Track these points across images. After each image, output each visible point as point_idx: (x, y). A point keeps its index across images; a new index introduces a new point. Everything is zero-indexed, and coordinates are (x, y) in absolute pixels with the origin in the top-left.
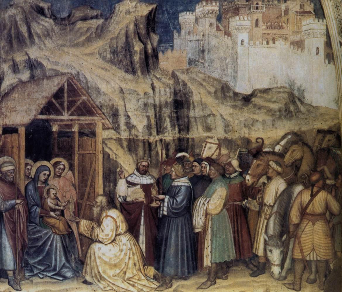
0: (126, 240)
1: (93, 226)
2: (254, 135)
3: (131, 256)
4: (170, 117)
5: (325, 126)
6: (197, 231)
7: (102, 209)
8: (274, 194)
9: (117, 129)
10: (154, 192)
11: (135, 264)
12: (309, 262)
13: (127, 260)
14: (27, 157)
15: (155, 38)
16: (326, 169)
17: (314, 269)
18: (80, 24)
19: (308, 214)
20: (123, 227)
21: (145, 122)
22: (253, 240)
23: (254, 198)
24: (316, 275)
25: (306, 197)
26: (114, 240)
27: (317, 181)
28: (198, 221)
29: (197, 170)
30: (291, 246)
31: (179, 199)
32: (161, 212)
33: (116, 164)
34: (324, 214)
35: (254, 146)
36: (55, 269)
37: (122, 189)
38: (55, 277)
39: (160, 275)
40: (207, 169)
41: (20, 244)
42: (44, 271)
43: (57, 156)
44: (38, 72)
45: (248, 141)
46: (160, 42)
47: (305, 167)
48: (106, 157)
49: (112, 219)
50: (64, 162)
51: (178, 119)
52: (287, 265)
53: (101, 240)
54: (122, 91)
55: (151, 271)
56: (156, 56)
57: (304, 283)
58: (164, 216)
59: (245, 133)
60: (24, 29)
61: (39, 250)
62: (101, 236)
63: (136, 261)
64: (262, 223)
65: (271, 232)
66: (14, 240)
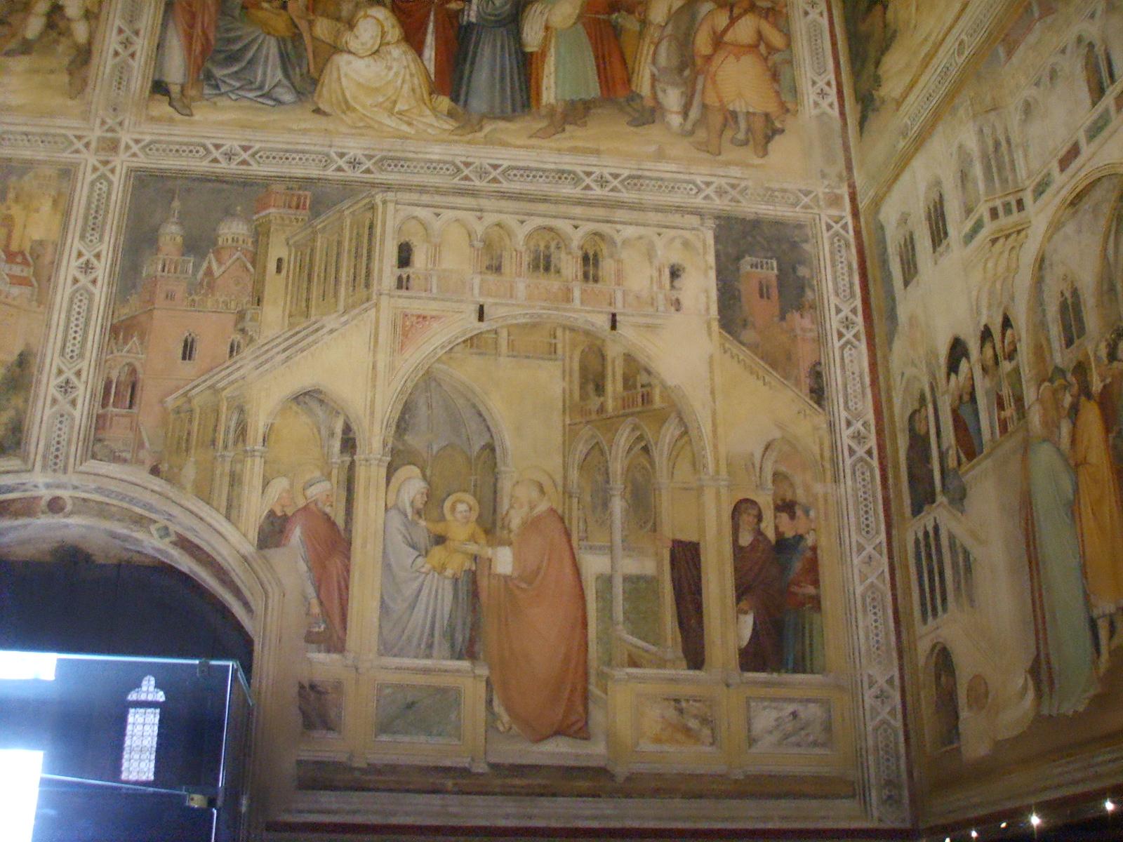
0: (399, 54)
1: (339, 29)
3: (408, 77)
6: (529, 49)
8: (666, 10)
11: (413, 90)
12: (734, 115)
13: (399, 82)
17: (743, 125)
19: (726, 43)
20: (394, 33)
22: (630, 71)
23: (630, 11)
24: (747, 133)
25: (722, 20)
26: (377, 51)
28: (532, 36)
30: (699, 87)
32: (466, 17)
36: (261, 88)
38: (260, 100)
39: (460, 109)
41: (199, 44)
42: (240, 88)
49: (374, 21)
52: (694, 113)
53: (353, 50)
55: (444, 102)
58: (470, 24)
61: (232, 58)
62: (354, 45)
63: (417, 87)
64: (646, 48)
65: (662, 60)
66: (189, 38)
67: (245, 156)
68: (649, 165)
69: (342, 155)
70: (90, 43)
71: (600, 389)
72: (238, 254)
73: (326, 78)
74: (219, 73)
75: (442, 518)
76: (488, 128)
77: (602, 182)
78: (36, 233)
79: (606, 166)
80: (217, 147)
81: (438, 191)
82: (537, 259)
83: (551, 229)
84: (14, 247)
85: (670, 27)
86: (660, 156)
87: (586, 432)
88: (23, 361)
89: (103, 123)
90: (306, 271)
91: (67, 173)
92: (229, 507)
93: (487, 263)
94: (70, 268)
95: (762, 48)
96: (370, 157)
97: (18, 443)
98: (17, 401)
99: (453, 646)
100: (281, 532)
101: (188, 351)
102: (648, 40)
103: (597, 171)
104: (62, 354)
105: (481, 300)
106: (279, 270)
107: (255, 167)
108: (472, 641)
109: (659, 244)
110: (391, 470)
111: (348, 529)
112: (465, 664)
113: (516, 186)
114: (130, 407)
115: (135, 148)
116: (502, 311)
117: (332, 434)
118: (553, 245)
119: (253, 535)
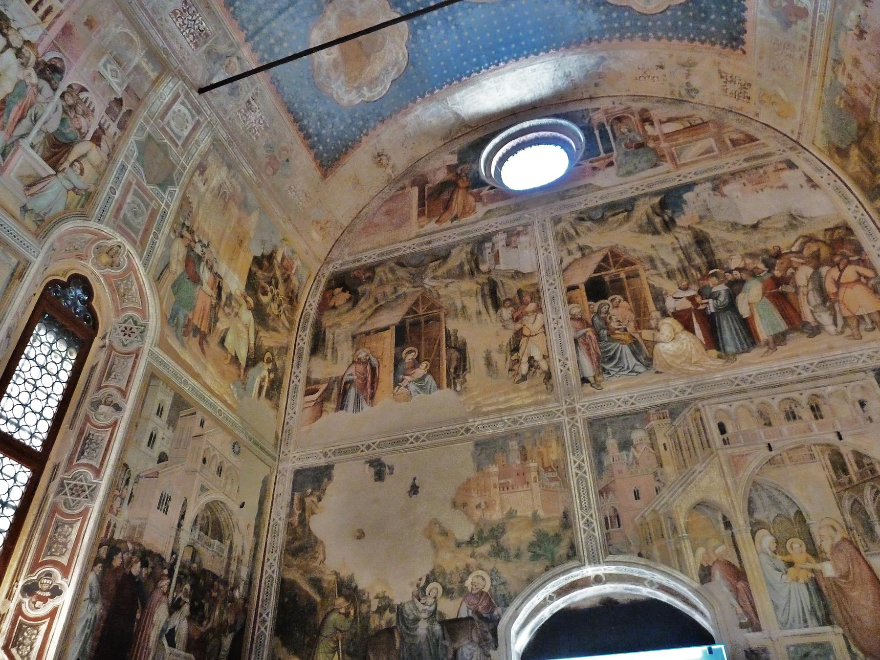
0: (685, 336)
2: (770, 246)
4: (696, 251)
5: (831, 225)
6: (745, 317)
7: (658, 320)
9: (655, 267)
10: (698, 299)
14: (589, 300)
15: (669, 212)
16: (845, 250)
17: (868, 320)
18: (610, 219)
20: (679, 327)
21: (677, 259)
23: (787, 284)
25: (835, 273)
27: (841, 260)
28: (744, 311)
29: (729, 277)
30: (837, 309)
31: (722, 298)
33: (661, 290)
34: (858, 281)
35: (773, 252)
36: (628, 368)
37: (671, 305)
40: (737, 275)
43: (612, 295)
44: (587, 251)
45: (766, 251)
46: (674, 212)
47: (825, 252)
48: (652, 287)
50: (619, 297)
51: (702, 251)
52: (840, 322)
54: (653, 246)
55: (714, 352)
56: (673, 221)
57: (863, 333)
59: (762, 246)
60: (572, 231)
61: (611, 359)
62: (662, 338)
65: (813, 302)
66: (590, 355)
67: (632, 401)
68: (827, 354)
69: (676, 389)
70: (549, 369)
71: (846, 471)
72: (644, 446)
73: (655, 357)
74: (607, 367)
75: (787, 553)
76: (740, 358)
77: (806, 369)
78: (554, 457)
79: (805, 361)
80: (619, 400)
81: (726, 394)
82: (787, 414)
83: (788, 399)
84: (546, 465)
85: (810, 284)
86: (831, 348)
87: (846, 494)
88: (566, 515)
89: (566, 402)
90: (679, 446)
91: (558, 427)
92: (681, 566)
93: (763, 422)
94: (572, 470)
95: (863, 280)
96: (689, 387)
97: (575, 554)
98: (568, 533)
99: (818, 619)
100: (710, 574)
101: (637, 496)
102: (801, 294)
103: (801, 364)
104: (581, 508)
105: (768, 441)
106: (666, 449)
107: (638, 405)
108: (827, 614)
109: (849, 393)
110: (753, 534)
111: (742, 567)
112: (828, 628)
113: (764, 382)
114: (619, 526)
115: (583, 409)
116: (779, 444)
117: (718, 521)
118: (793, 406)
119: (696, 577)
